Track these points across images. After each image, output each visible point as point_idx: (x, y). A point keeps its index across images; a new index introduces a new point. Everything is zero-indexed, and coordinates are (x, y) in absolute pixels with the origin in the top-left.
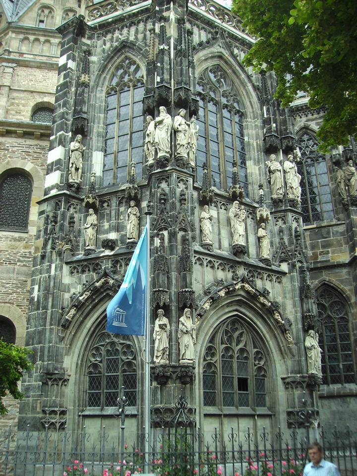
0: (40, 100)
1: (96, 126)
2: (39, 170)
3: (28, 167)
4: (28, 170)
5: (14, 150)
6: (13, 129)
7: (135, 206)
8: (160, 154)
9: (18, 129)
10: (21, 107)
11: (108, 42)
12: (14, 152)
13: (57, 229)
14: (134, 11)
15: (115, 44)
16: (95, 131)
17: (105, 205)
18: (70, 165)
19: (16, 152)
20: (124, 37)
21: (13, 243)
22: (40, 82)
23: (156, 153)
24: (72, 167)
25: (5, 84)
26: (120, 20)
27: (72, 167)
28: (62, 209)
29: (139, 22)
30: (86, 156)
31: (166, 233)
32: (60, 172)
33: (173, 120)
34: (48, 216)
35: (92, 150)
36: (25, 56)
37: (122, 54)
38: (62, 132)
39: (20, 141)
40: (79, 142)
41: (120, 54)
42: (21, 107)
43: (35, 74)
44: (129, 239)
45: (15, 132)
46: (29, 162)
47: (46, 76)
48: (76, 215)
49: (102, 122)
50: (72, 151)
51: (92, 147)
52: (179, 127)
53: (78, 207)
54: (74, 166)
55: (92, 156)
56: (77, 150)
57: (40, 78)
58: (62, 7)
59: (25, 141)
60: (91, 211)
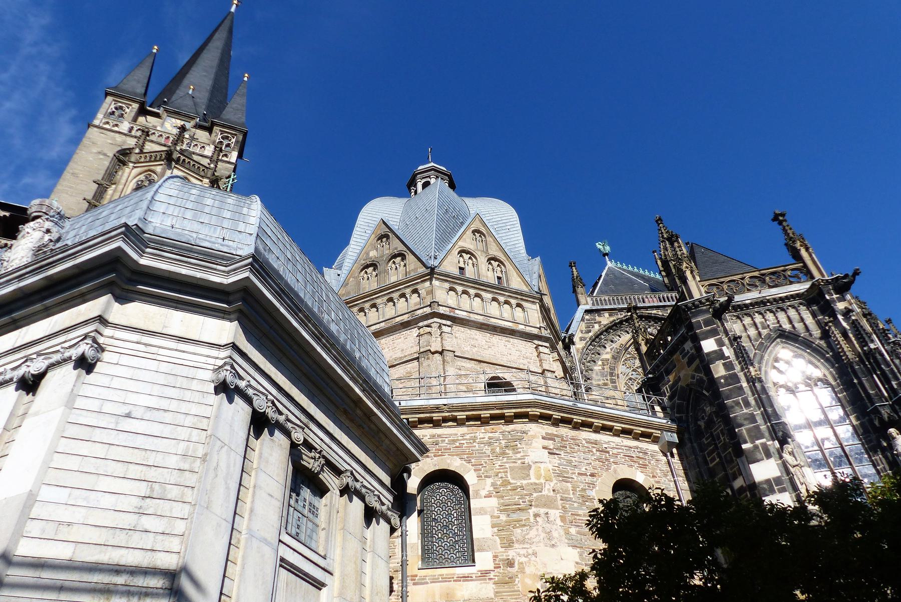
12: (616, 455)
15: (765, 332)
19: (619, 456)
25: (447, 348)
26: (762, 303)
36: (457, 312)
43: (476, 337)
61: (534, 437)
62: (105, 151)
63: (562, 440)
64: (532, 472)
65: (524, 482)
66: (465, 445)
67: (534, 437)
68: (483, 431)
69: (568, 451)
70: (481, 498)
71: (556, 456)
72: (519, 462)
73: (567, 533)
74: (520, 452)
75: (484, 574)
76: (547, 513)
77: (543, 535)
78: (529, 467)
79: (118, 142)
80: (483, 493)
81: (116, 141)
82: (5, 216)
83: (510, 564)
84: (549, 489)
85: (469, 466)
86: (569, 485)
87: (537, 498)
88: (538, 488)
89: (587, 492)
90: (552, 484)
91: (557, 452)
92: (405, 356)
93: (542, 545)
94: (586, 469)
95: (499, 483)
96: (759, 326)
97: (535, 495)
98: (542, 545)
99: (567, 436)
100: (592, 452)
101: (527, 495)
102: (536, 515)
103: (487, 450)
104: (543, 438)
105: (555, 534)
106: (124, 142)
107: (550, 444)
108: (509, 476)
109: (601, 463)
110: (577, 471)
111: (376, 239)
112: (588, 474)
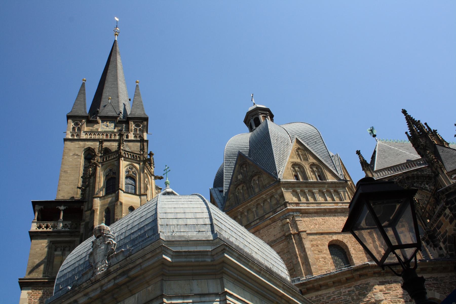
0: (331, 239)
10: (321, 247)
22: (322, 224)
25: (301, 230)
42: (321, 247)
62: (77, 153)
66: (336, 298)
69: (394, 289)
79: (81, 145)
81: (80, 145)
82: (41, 208)
92: (277, 239)
94: (406, 298)
99: (391, 281)
103: (348, 298)
111: (239, 167)
112: (408, 300)
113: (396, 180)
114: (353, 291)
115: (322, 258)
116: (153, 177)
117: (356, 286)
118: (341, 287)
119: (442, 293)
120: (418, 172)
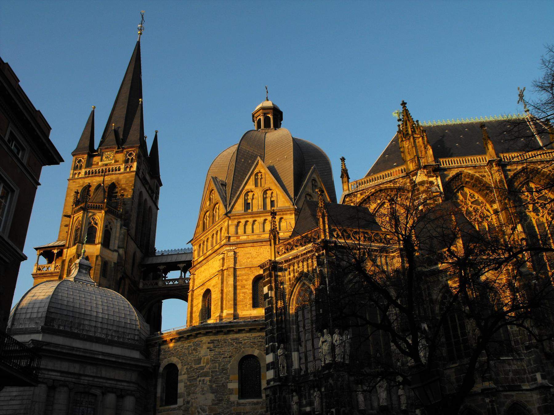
0: (258, 274)
1: (292, 334)
2: (263, 354)
3: (256, 353)
4: (256, 355)
5: (245, 342)
6: (243, 328)
7: (318, 390)
8: (327, 362)
9: (245, 328)
11: (292, 272)
12: (245, 343)
13: (277, 406)
14: (304, 252)
16: (291, 338)
17: (302, 388)
18: (279, 366)
20: (301, 269)
21: (254, 406)
22: (255, 258)
23: (325, 361)
24: (280, 366)
27: (280, 366)
28: (278, 394)
29: (308, 258)
30: (288, 357)
31: (333, 410)
32: (274, 370)
33: (332, 337)
34: (271, 398)
35: (291, 351)
37: (301, 281)
38: (271, 343)
39: (248, 335)
40: (283, 349)
41: (299, 281)
43: (251, 252)
44: (317, 412)
45: (244, 330)
46: (256, 350)
47: (258, 252)
48: (287, 396)
49: (295, 331)
50: (279, 356)
51: (291, 349)
52: (335, 343)
53: (287, 390)
54: (282, 365)
55: (292, 355)
56: (282, 355)
57: (254, 255)
58: (261, 190)
59: (251, 335)
60: (294, 394)
61: (204, 343)
63: (218, 342)
64: (202, 361)
65: (198, 366)
66: (180, 351)
67: (204, 343)
68: (186, 343)
69: (220, 347)
70: (182, 375)
71: (213, 351)
72: (197, 357)
73: (211, 387)
74: (197, 352)
75: (180, 407)
76: (203, 380)
77: (201, 390)
78: (201, 359)
80: (183, 373)
83: (188, 402)
84: (207, 369)
85: (179, 361)
86: (217, 364)
87: (201, 373)
88: (202, 368)
89: (225, 366)
90: (209, 366)
91: (214, 349)
93: (199, 394)
95: (188, 368)
96: (295, 270)
97: (201, 371)
98: (199, 394)
100: (233, 344)
101: (197, 372)
102: (200, 381)
103: (187, 352)
104: (209, 343)
105: (205, 389)
106: (84, 183)
107: (211, 345)
108: (193, 364)
109: (236, 350)
110: (223, 356)
113: (368, 193)
114: (191, 346)
115: (243, 293)
116: (119, 220)
117: (194, 342)
118: (184, 343)
119: (262, 351)
120: (391, 184)
